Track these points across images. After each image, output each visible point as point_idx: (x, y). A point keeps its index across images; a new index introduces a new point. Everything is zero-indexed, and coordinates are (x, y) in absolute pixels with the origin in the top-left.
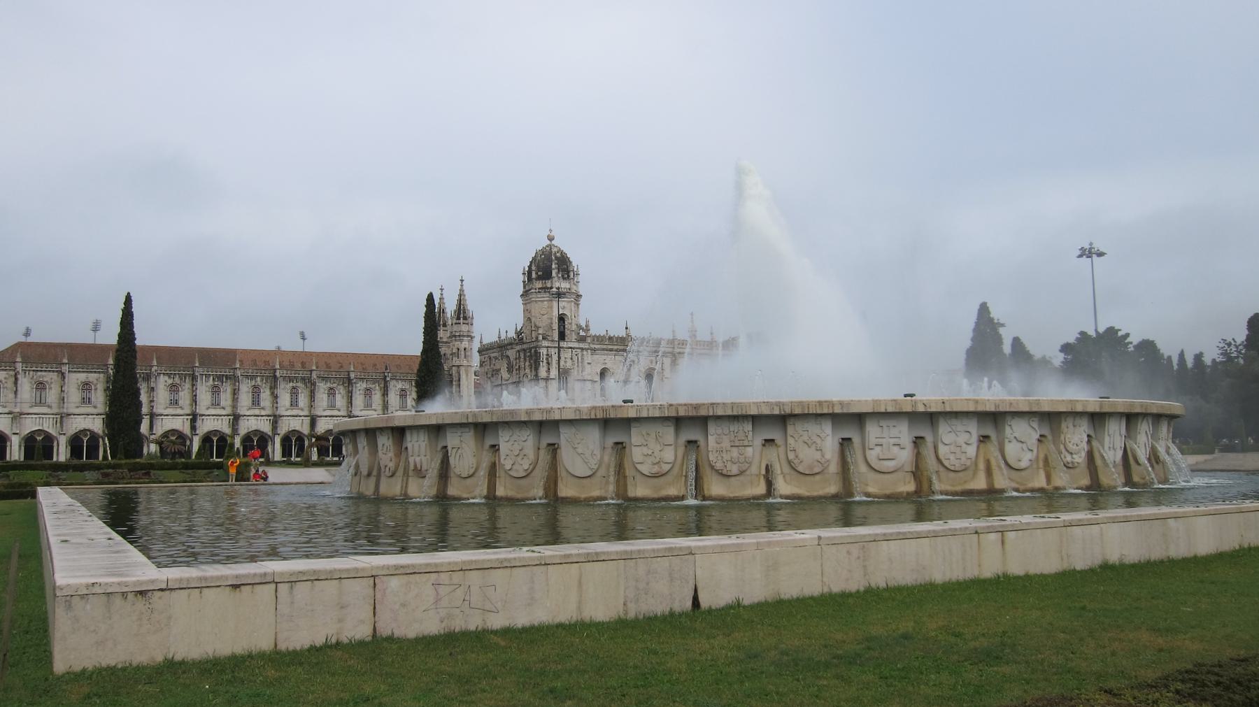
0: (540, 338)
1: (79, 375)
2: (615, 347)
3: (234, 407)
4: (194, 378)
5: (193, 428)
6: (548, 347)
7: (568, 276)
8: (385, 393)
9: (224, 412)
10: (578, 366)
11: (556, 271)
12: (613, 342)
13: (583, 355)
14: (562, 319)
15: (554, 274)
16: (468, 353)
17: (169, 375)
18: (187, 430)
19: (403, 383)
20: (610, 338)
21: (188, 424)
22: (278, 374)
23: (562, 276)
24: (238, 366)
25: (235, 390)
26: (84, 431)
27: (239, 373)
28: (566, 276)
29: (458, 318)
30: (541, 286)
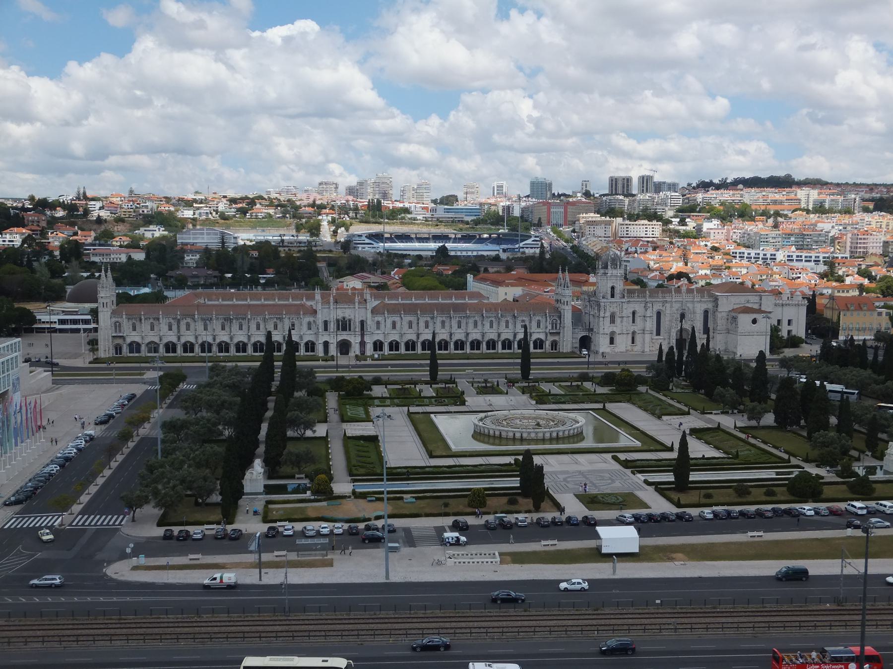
0: (601, 298)
3: (466, 329)
4: (451, 318)
5: (451, 339)
9: (463, 332)
14: (613, 288)
15: (609, 267)
16: (569, 303)
17: (441, 317)
18: (448, 339)
21: (449, 336)
22: (484, 315)
24: (468, 312)
26: (410, 340)
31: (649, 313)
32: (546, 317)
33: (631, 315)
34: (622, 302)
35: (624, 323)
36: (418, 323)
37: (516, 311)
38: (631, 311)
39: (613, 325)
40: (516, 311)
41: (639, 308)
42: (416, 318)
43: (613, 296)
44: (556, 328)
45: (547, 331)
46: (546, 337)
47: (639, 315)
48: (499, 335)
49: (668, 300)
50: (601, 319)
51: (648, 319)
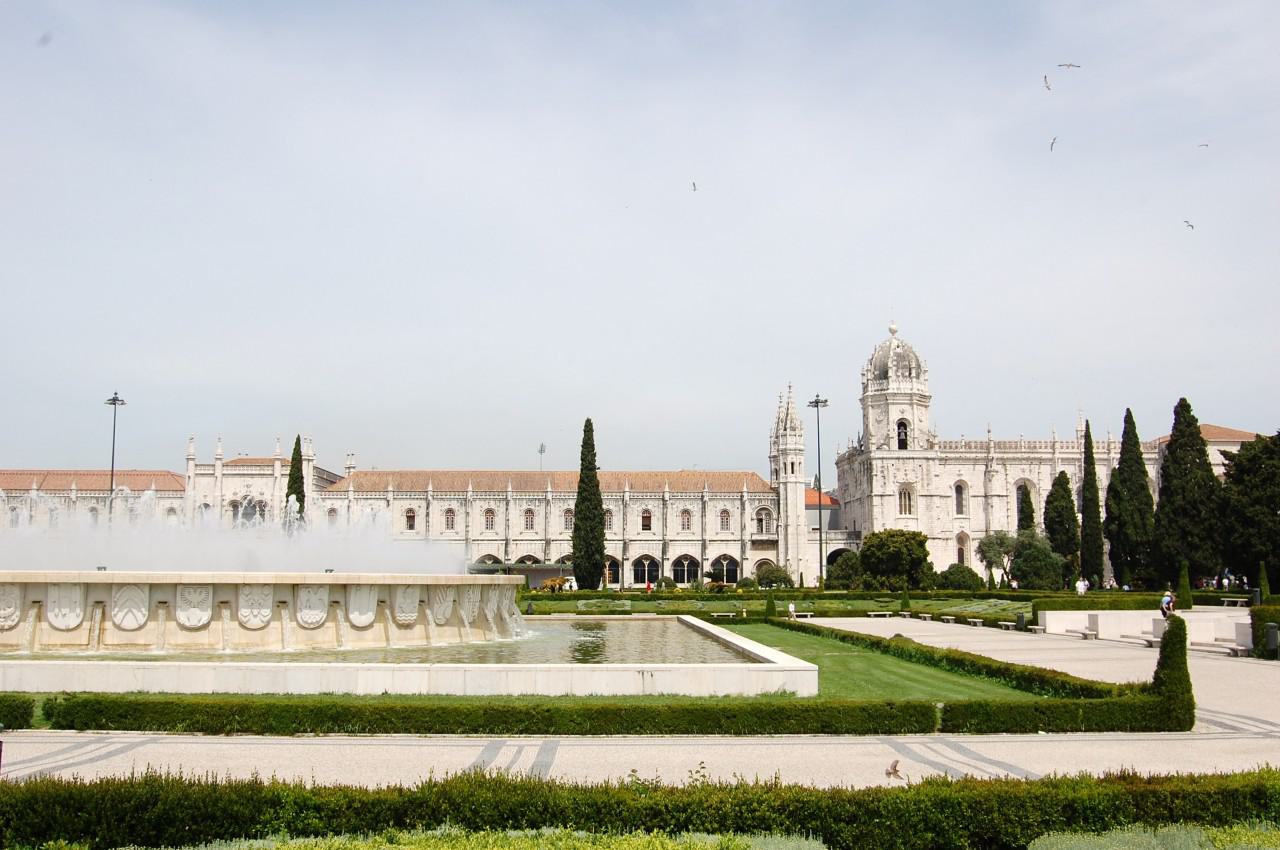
1: (402, 502)
2: (973, 455)
6: (883, 458)
7: (910, 374)
8: (703, 515)
10: (922, 479)
11: (894, 368)
12: (970, 448)
13: (928, 466)
14: (902, 425)
15: (890, 374)
16: (795, 468)
19: (726, 503)
20: (968, 445)
23: (902, 374)
25: (546, 513)
27: (549, 496)
28: (907, 374)
29: (785, 430)
30: (876, 388)
31: (998, 485)
32: (743, 504)
33: (953, 494)
34: (928, 459)
35: (935, 514)
36: (428, 515)
37: (667, 489)
38: (952, 483)
39: (908, 516)
40: (667, 489)
41: (973, 476)
42: (424, 504)
43: (903, 445)
44: (768, 531)
45: (747, 537)
46: (743, 552)
47: (972, 493)
48: (625, 549)
49: (1045, 456)
50: (876, 501)
51: (995, 501)
